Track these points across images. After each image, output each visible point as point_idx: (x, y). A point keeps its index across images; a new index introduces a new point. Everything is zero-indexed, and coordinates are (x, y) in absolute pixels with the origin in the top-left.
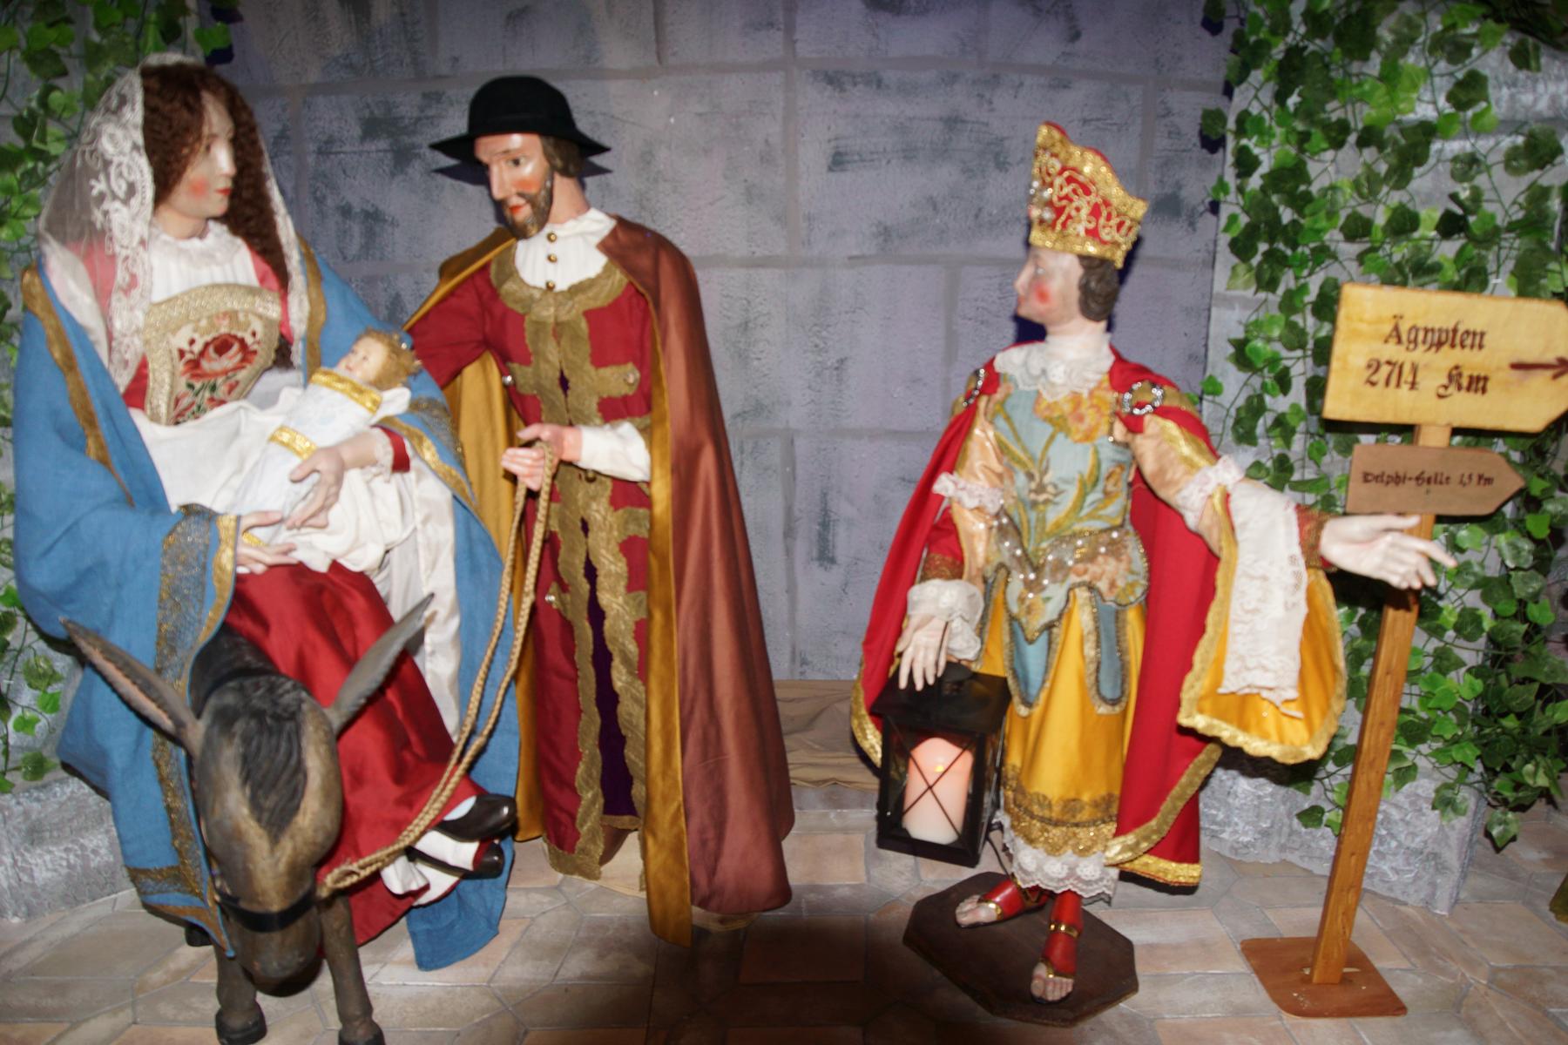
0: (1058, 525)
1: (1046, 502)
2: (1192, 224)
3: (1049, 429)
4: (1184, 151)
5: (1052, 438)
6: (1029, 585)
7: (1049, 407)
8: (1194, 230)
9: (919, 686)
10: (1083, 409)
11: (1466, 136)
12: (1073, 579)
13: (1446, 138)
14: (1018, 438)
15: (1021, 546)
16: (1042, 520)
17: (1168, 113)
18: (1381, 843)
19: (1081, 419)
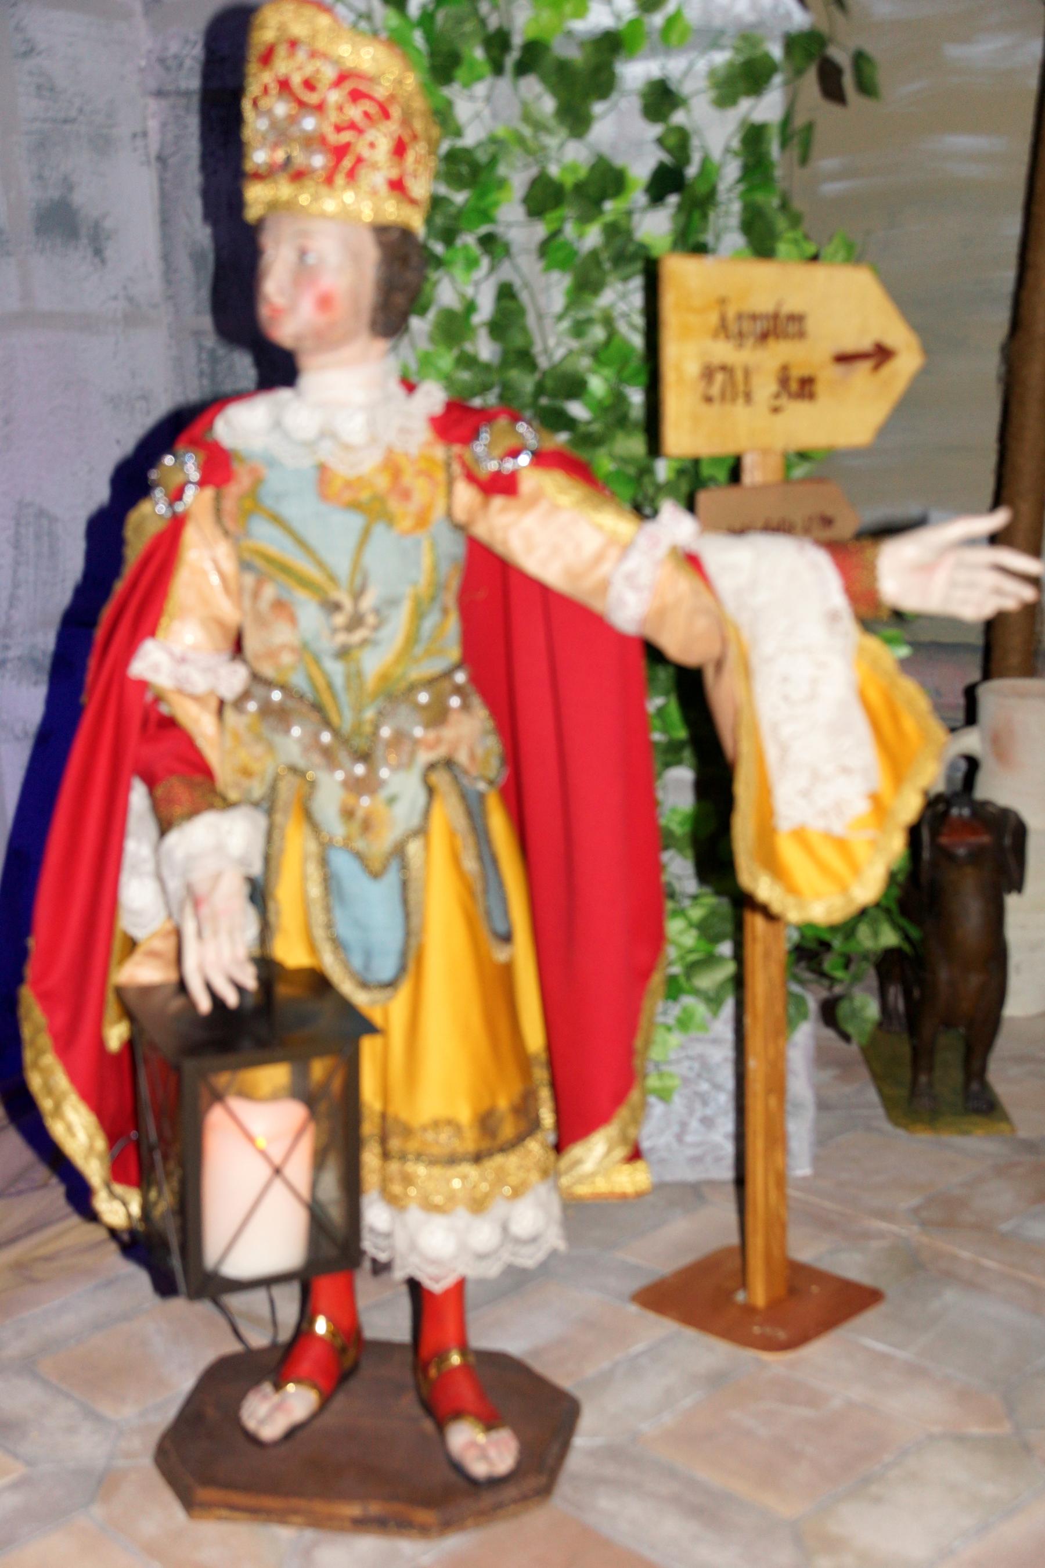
0: (384, 677)
1: (364, 642)
2: (98, 252)
3: (355, 521)
4: (66, 121)
5: (365, 535)
6: (357, 786)
7: (348, 485)
8: (103, 262)
9: (232, 999)
10: (408, 479)
11: (653, 53)
12: (424, 757)
13: (631, 57)
14: (301, 542)
15: (327, 724)
16: (355, 677)
17: (30, 51)
18: (705, 1103)
19: (406, 495)
